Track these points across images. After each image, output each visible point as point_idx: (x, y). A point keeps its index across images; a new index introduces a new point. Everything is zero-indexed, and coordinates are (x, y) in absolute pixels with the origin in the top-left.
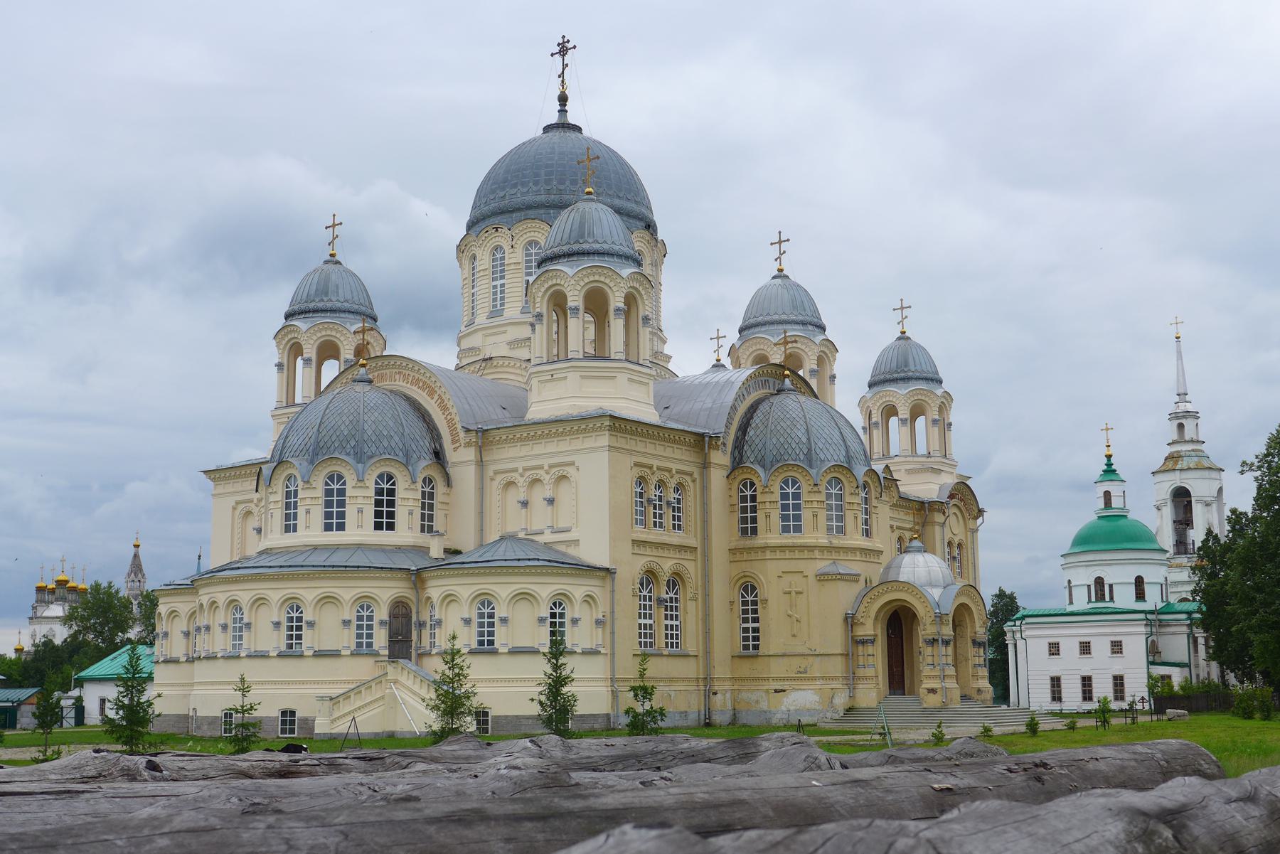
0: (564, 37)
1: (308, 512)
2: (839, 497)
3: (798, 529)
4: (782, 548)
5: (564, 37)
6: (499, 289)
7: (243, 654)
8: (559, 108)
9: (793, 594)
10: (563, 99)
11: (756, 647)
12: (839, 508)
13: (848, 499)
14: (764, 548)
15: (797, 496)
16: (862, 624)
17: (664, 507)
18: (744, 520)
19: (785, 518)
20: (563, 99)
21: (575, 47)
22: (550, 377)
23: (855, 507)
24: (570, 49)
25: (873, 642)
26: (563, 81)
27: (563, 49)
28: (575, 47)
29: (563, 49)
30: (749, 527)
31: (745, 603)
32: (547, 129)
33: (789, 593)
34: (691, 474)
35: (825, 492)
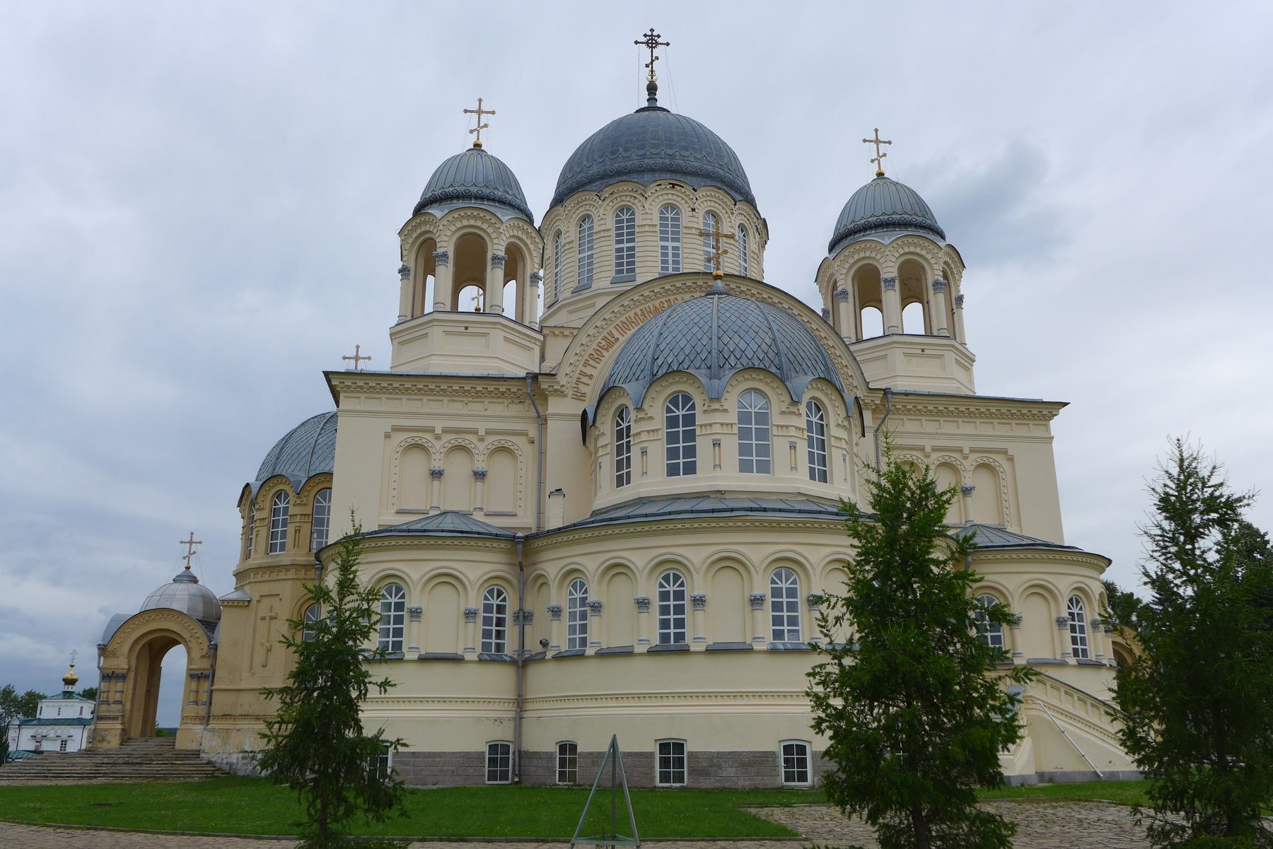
0: (652, 30)
1: (644, 452)
6: (670, 251)
7: (590, 651)
8: (648, 97)
10: (652, 89)
20: (652, 89)
21: (668, 44)
24: (661, 44)
26: (652, 71)
28: (668, 44)
29: (652, 41)
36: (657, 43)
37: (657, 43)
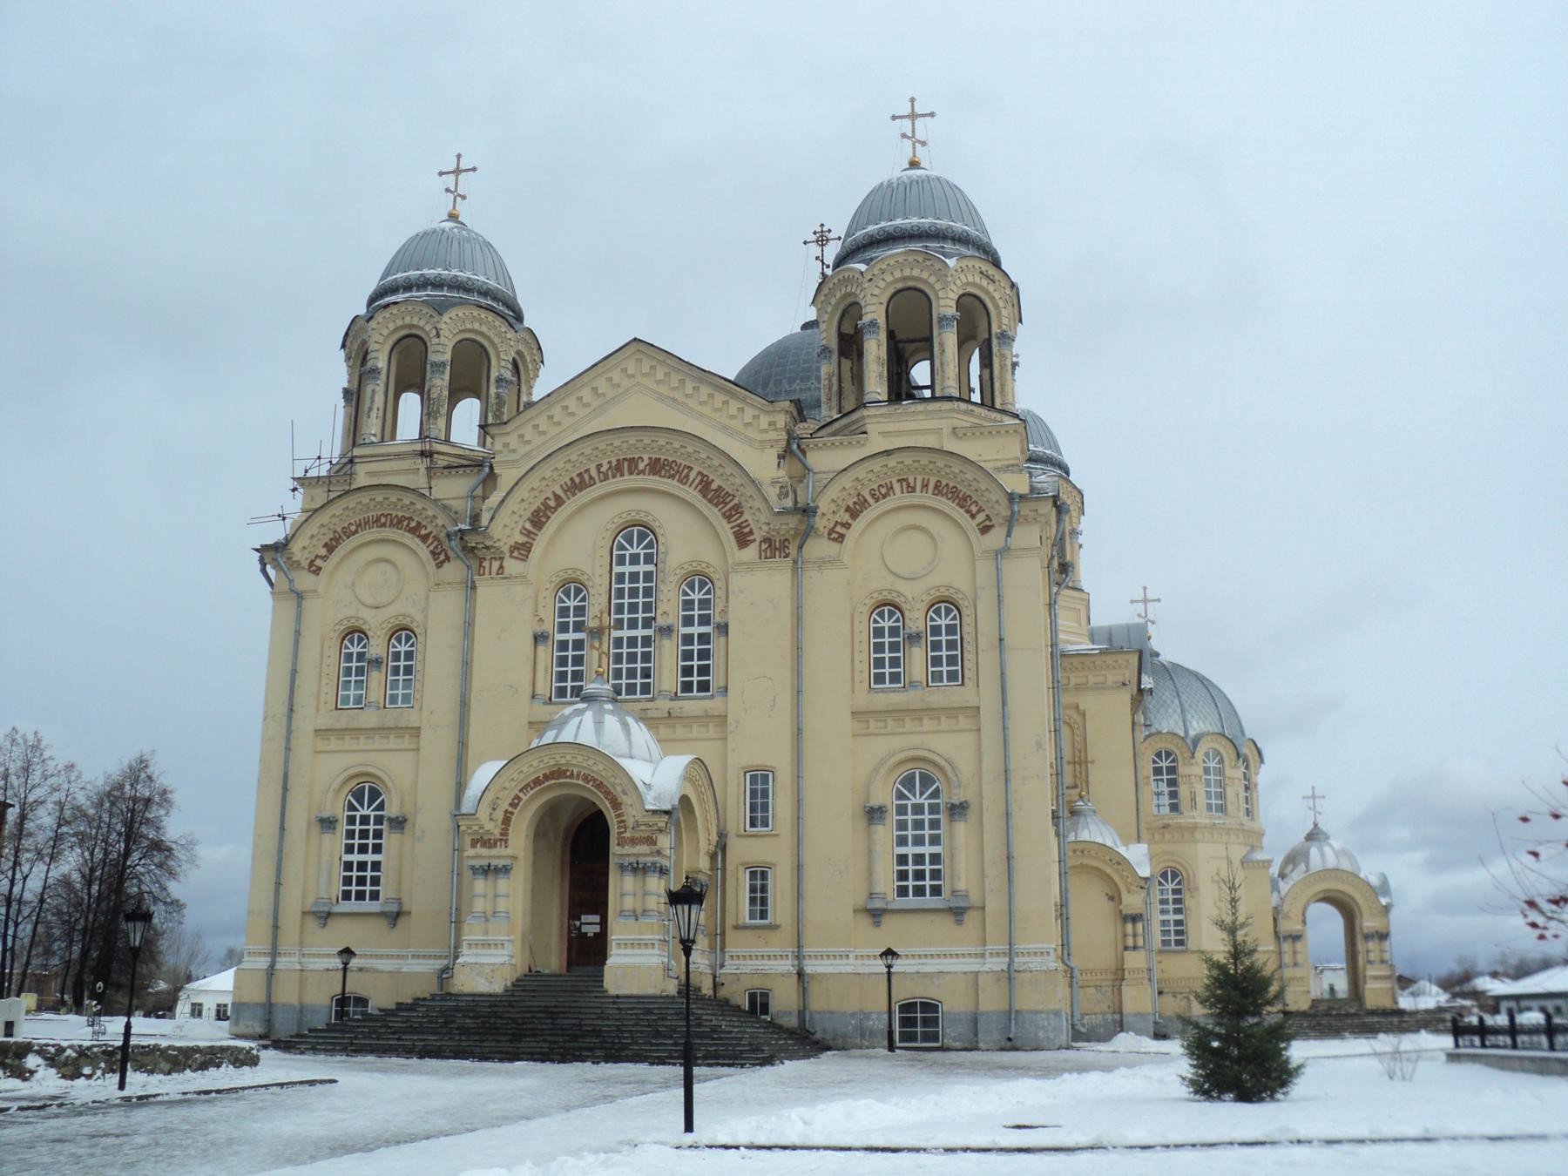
0: (822, 225)
5: (822, 225)
11: (1180, 943)
12: (1220, 784)
15: (1220, 772)
32: (806, 326)
36: (827, 240)
37: (827, 240)
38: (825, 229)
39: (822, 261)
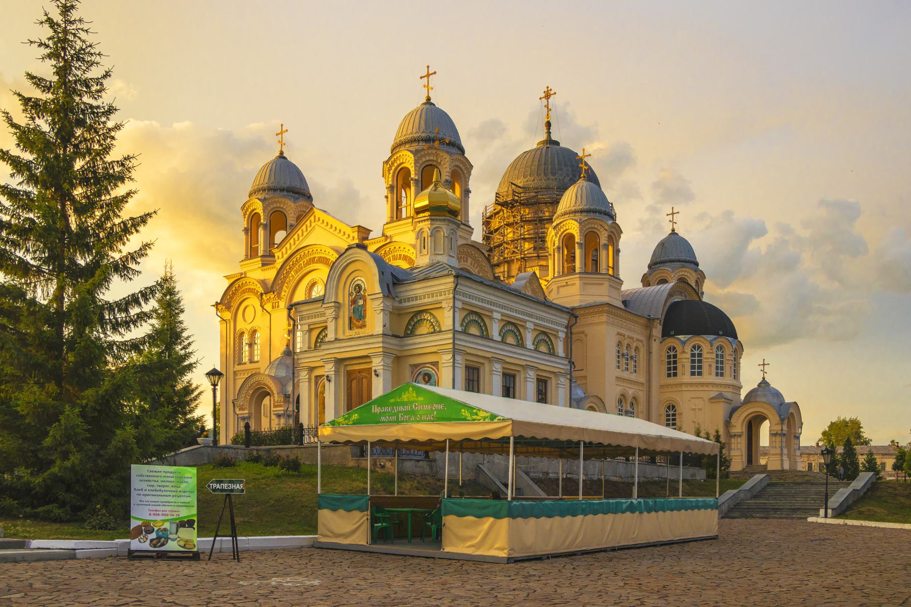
0: (548, 87)
2: (722, 356)
3: (700, 374)
4: (691, 384)
5: (548, 87)
9: (697, 410)
10: (549, 125)
13: (728, 357)
14: (681, 384)
15: (700, 355)
16: (735, 426)
17: (629, 359)
18: (669, 369)
19: (693, 367)
20: (549, 125)
21: (555, 93)
22: (565, 284)
23: (730, 362)
24: (552, 94)
25: (740, 436)
27: (548, 95)
28: (555, 93)
29: (548, 95)
30: (672, 371)
31: (668, 415)
33: (694, 409)
34: (642, 342)
35: (715, 353)
36: (550, 95)
38: (549, 89)
39: (548, 107)
